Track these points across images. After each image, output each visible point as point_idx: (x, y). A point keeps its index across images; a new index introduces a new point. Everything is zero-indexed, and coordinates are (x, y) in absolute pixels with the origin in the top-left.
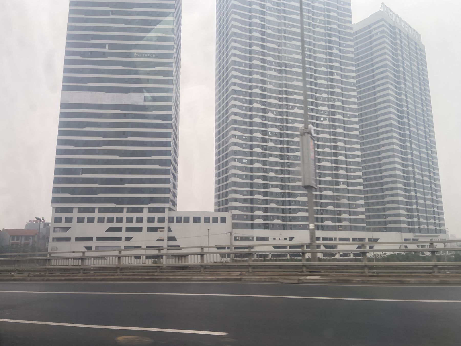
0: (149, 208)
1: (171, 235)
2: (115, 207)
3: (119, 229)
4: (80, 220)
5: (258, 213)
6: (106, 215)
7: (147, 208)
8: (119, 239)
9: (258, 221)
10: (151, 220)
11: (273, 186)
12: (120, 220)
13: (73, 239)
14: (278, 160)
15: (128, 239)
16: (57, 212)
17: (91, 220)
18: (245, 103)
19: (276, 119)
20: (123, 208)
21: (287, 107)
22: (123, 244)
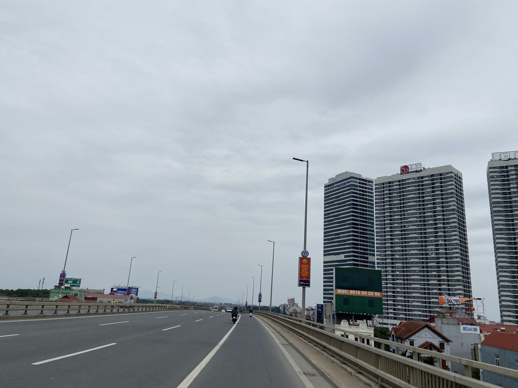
5: (390, 311)
9: (390, 315)
11: (399, 296)
14: (402, 281)
18: (383, 252)
19: (400, 258)
21: (406, 251)
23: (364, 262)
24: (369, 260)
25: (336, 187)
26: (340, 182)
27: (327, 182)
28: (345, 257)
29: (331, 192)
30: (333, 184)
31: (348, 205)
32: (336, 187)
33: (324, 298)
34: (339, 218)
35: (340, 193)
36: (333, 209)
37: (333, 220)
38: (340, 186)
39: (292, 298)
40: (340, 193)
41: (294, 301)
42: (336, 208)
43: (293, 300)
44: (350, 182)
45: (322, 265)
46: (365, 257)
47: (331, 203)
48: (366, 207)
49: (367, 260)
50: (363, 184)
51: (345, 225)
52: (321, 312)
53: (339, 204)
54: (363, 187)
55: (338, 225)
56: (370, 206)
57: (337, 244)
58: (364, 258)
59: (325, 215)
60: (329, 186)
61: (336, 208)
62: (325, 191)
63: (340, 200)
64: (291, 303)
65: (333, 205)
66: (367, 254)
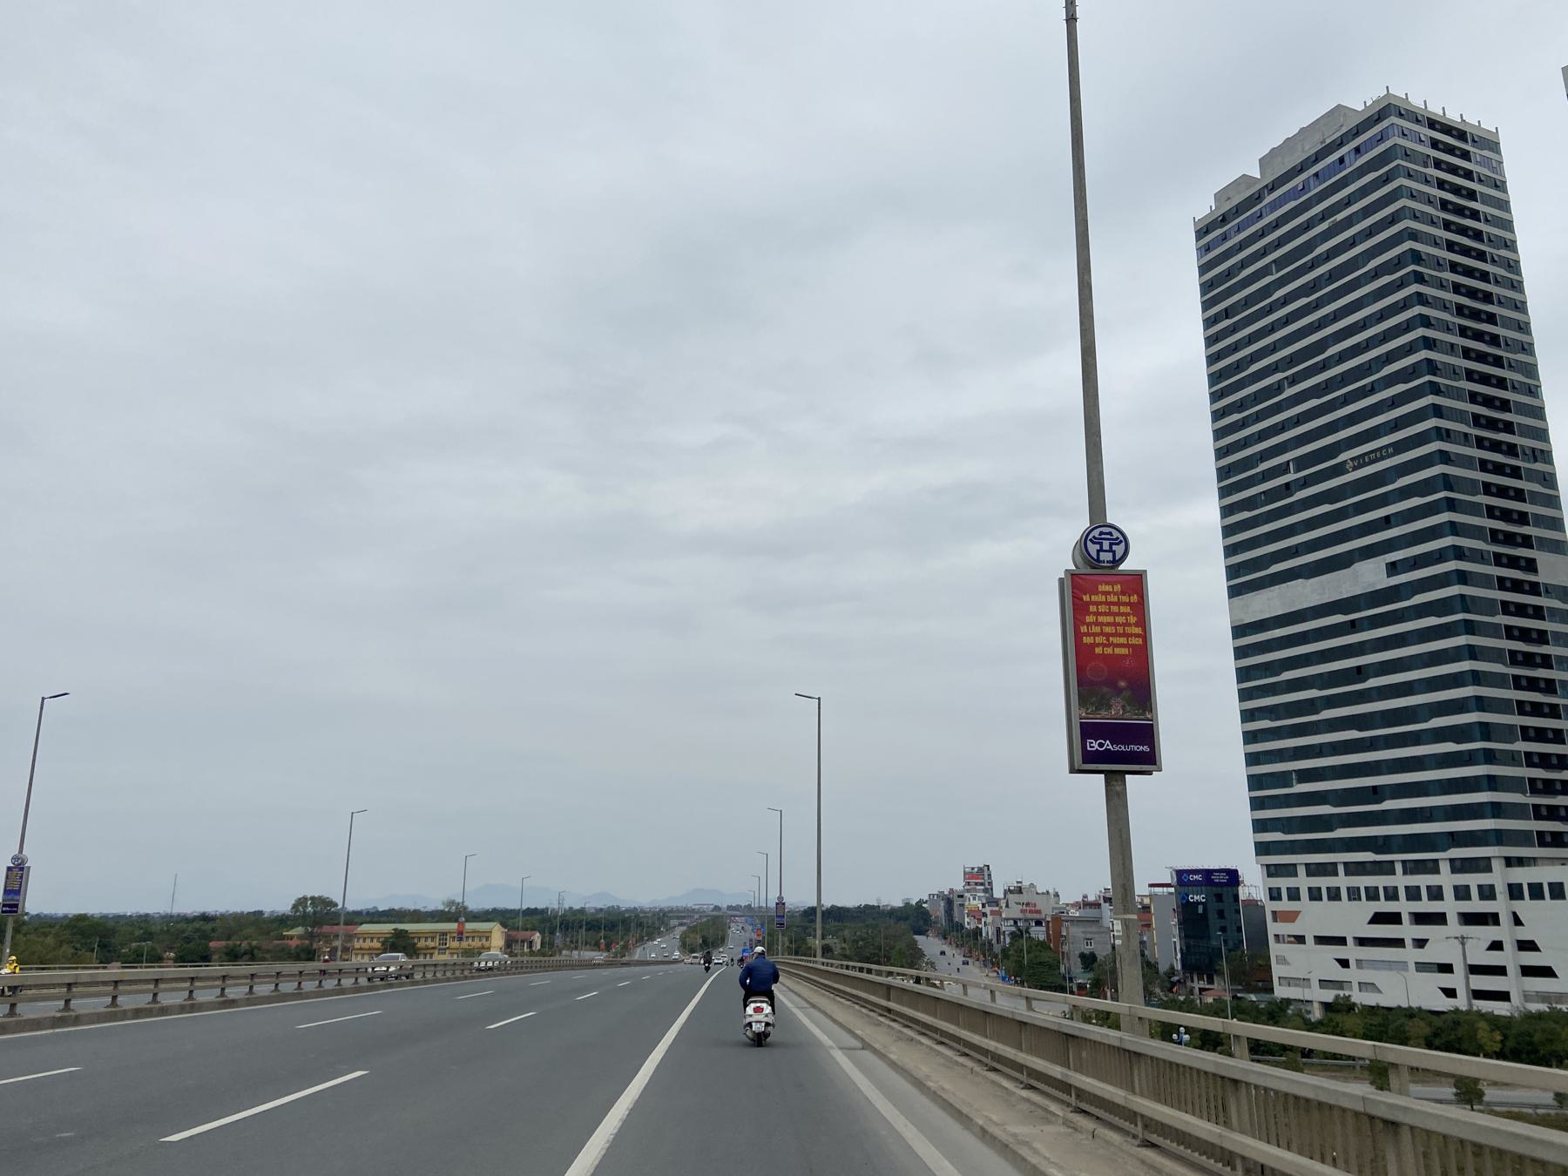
0: (1452, 861)
1: (1524, 934)
2: (1375, 862)
3: (1394, 918)
4: (1315, 895)
6: (1363, 882)
7: (1448, 862)
8: (1399, 943)
10: (1462, 893)
12: (1392, 894)
13: (1310, 940)
15: (1421, 943)
16: (1270, 875)
17: (1334, 895)
20: (1392, 862)
22: (1410, 954)
23: (1517, 586)
24: (1542, 578)
25: (1274, 206)
26: (1300, 169)
27: (1204, 206)
28: (1393, 568)
29: (1242, 246)
30: (1258, 197)
31: (1376, 274)
32: (1274, 206)
33: (1260, 826)
34: (1324, 366)
35: (1308, 226)
36: (1272, 329)
37: (1278, 388)
38: (1305, 188)
39: (982, 866)
40: (1308, 226)
41: (990, 875)
42: (1287, 321)
43: (986, 873)
44: (1381, 138)
45: (1228, 644)
46: (1518, 558)
47: (1247, 302)
48: (1484, 277)
49: (1531, 578)
50: (1450, 150)
51: (1372, 389)
52: (1205, 909)
53: (1314, 286)
54: (1453, 170)
55: (1313, 403)
56: (1501, 272)
57: (1326, 508)
58: (1513, 562)
59: (1214, 378)
60: (1224, 219)
61: (1287, 321)
62: (1200, 257)
63: (1313, 265)
64: (976, 884)
65: (1270, 309)
66: (1527, 542)
